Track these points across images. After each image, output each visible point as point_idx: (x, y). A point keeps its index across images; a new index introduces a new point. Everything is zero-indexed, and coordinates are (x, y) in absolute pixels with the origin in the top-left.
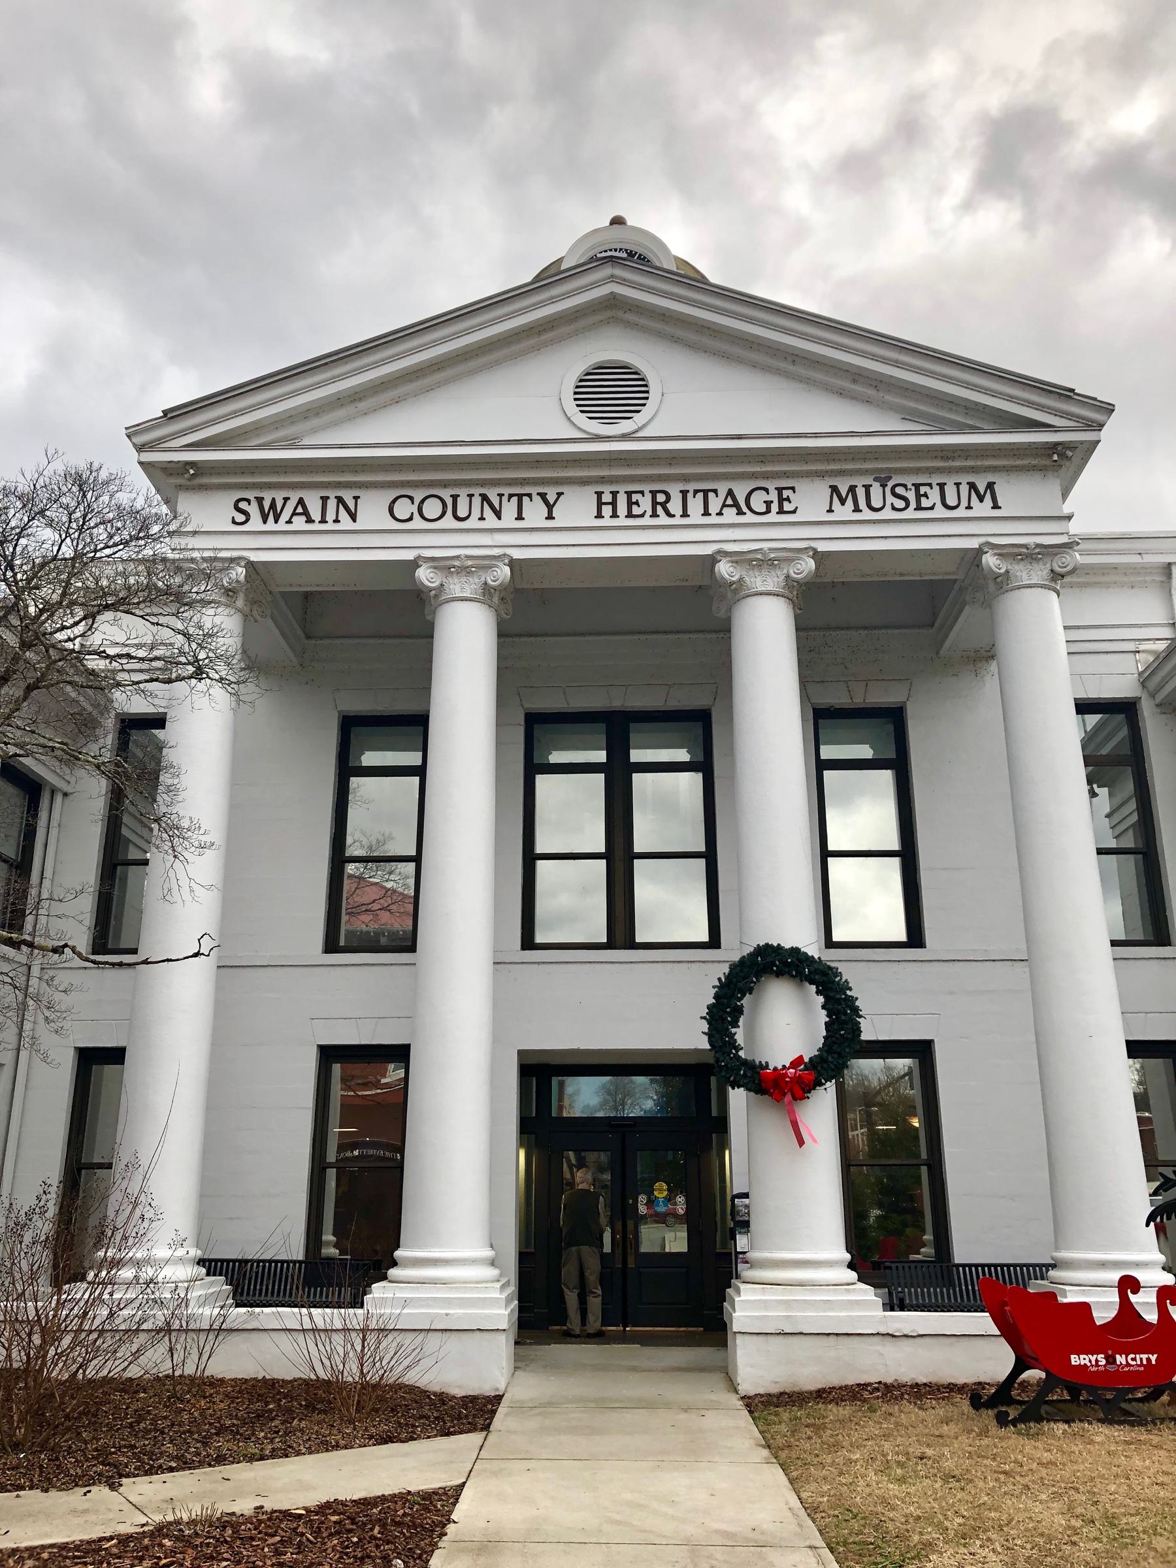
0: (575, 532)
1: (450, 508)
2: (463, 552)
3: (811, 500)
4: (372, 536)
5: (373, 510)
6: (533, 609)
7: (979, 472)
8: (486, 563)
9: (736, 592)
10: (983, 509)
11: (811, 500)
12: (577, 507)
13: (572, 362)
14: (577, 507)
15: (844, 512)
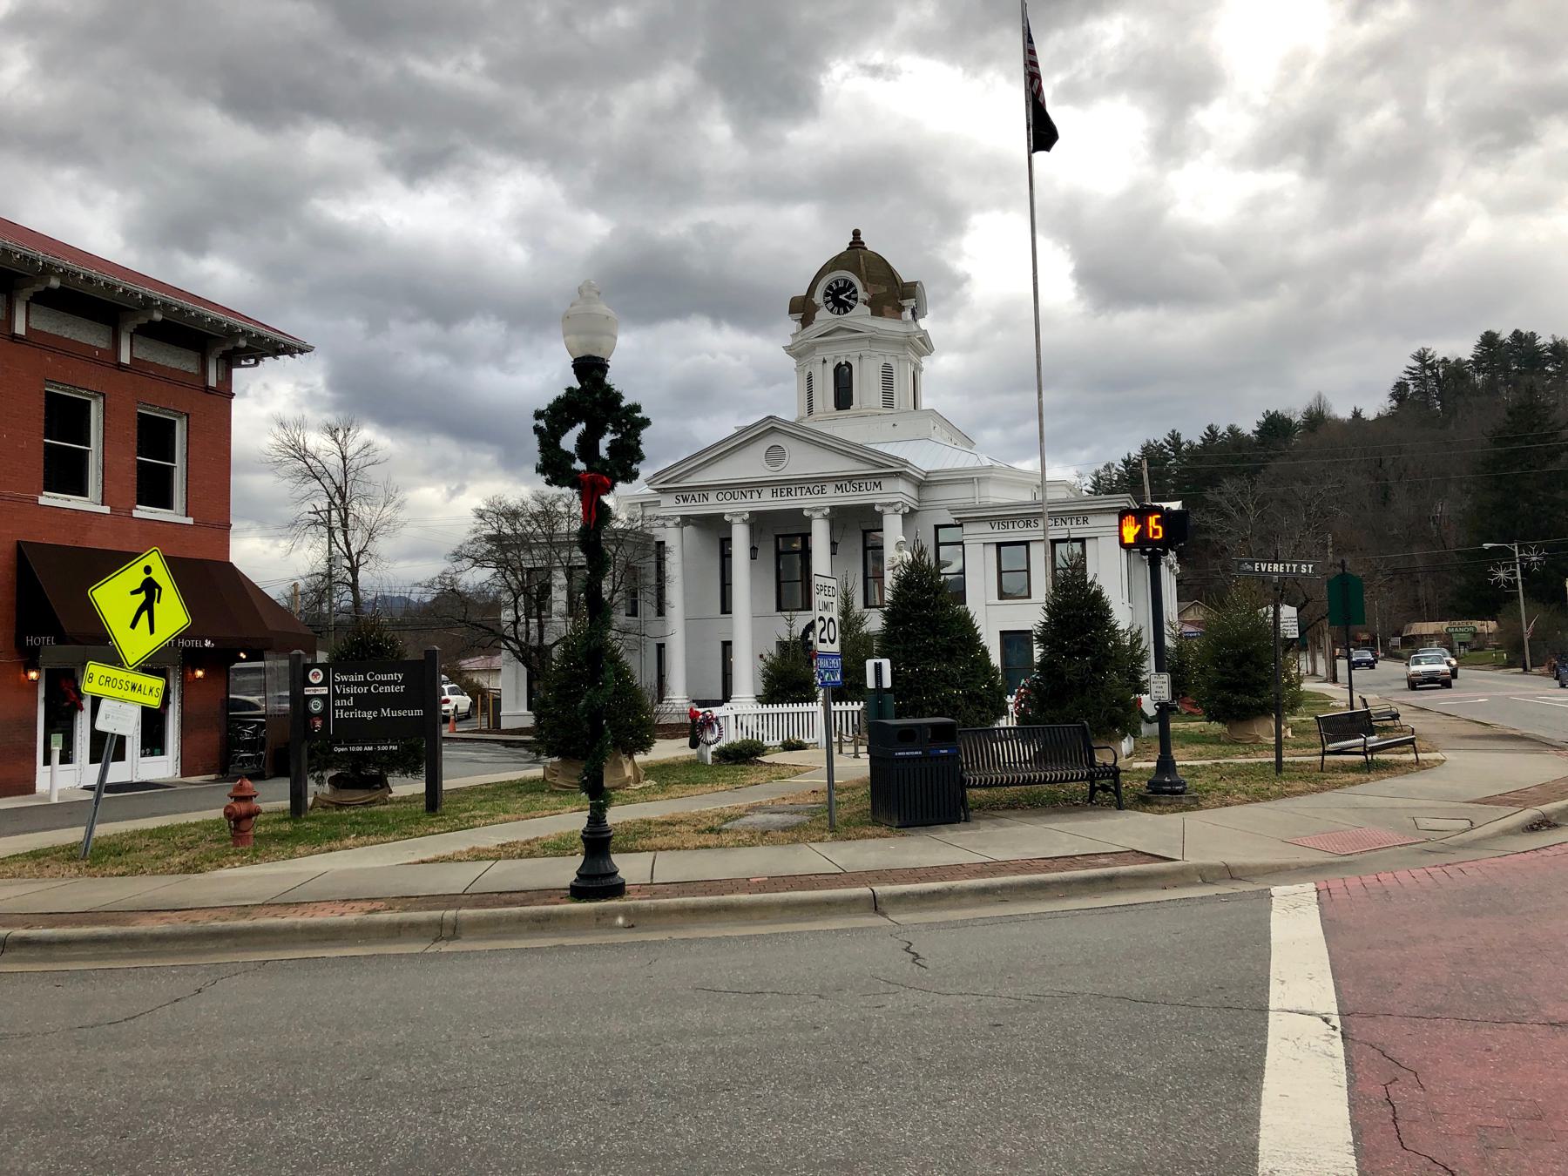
0: (767, 502)
1: (732, 496)
2: (736, 509)
3: (830, 489)
4: (711, 505)
5: (712, 496)
6: (759, 523)
7: (876, 479)
8: (742, 513)
9: (809, 520)
10: (877, 490)
11: (830, 489)
12: (767, 494)
13: (762, 447)
14: (767, 494)
15: (839, 493)
